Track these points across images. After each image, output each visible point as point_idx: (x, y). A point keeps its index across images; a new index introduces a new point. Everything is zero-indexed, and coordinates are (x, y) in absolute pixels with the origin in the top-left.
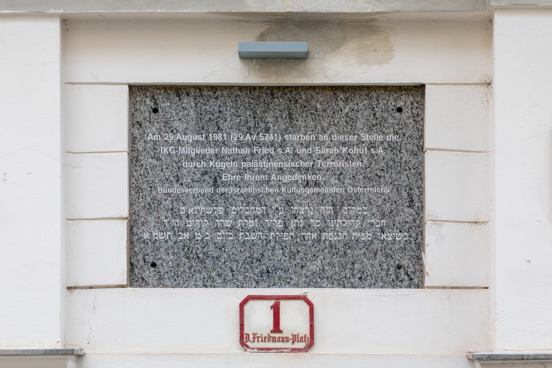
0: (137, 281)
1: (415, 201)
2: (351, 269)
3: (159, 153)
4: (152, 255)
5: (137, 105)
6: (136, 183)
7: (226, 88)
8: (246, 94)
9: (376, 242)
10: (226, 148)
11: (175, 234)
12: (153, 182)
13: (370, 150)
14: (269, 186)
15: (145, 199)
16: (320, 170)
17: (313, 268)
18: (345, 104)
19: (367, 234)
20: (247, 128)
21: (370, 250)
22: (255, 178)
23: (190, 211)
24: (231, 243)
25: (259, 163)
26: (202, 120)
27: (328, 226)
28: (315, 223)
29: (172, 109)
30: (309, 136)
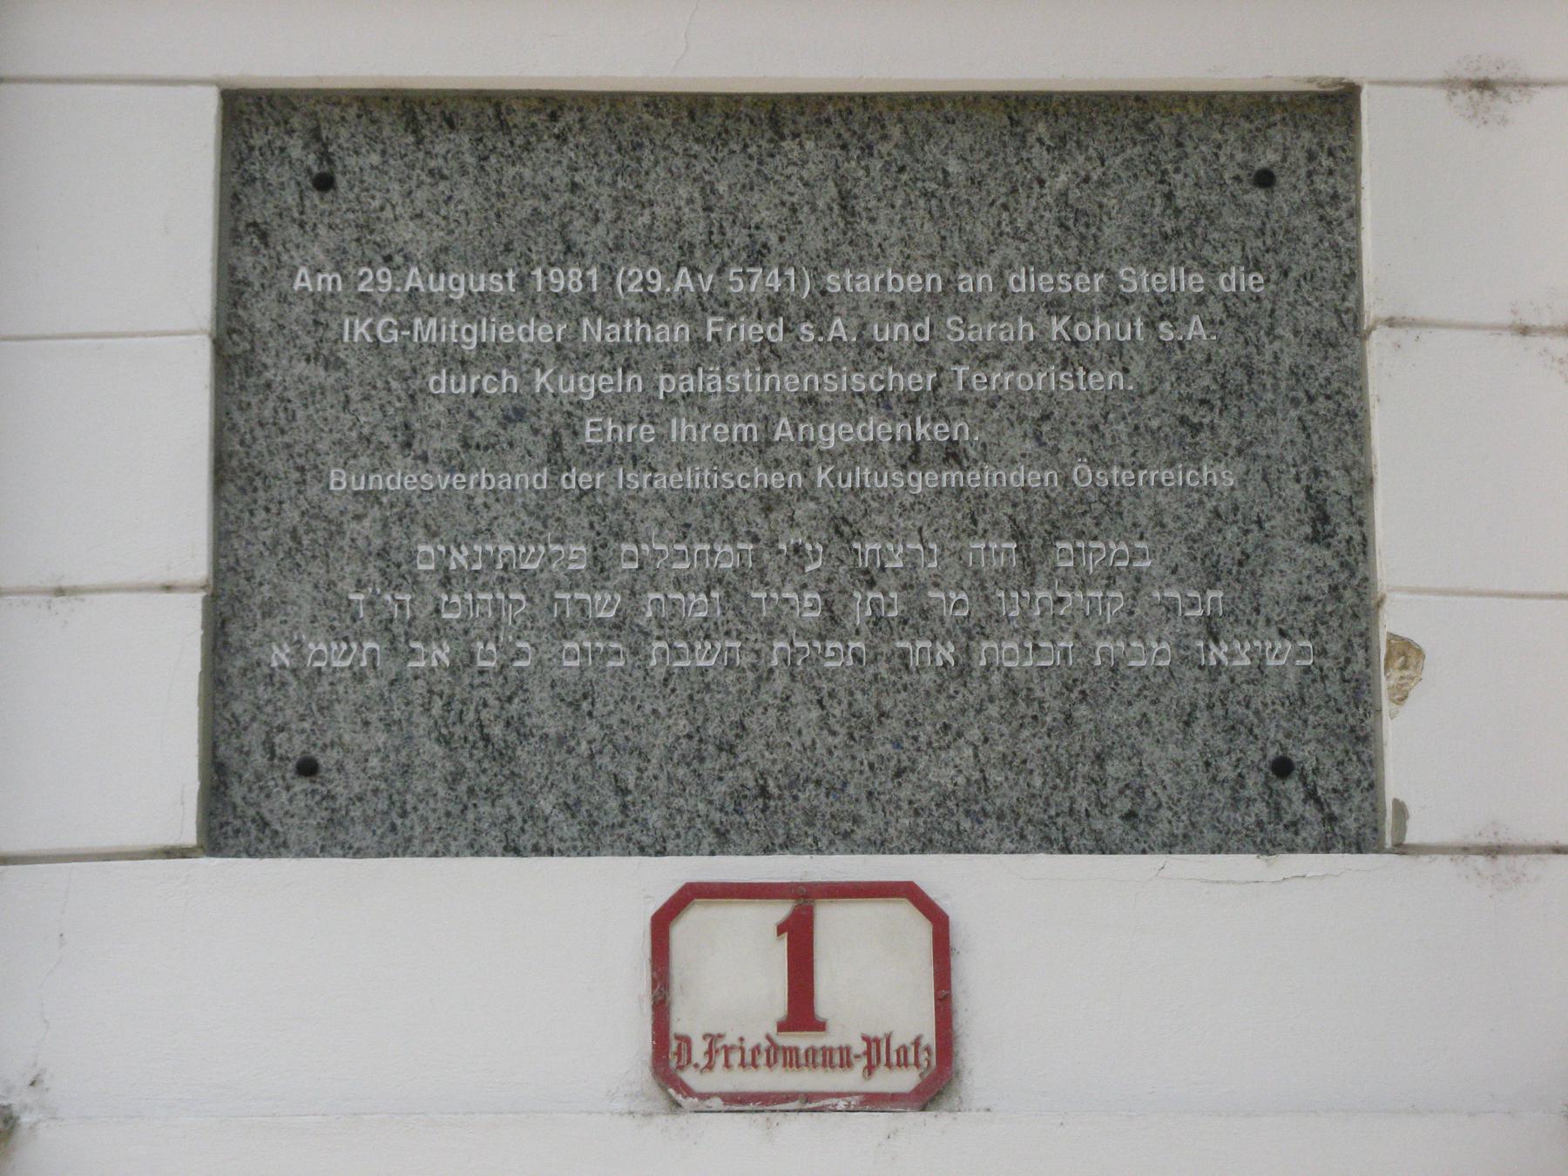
1: (1334, 520)
2: (1093, 780)
3: (336, 342)
4: (303, 731)
5: (253, 164)
6: (243, 455)
8: (676, 122)
9: (1190, 674)
10: (600, 320)
11: (395, 649)
12: (311, 448)
13: (1156, 329)
15: (279, 514)
16: (963, 402)
17: (943, 776)
18: (1054, 158)
19: (1154, 645)
20: (680, 248)
22: (709, 433)
23: (455, 559)
24: (615, 682)
25: (728, 378)
26: (504, 216)
27: (998, 613)
28: (949, 601)
29: (386, 178)
30: (918, 277)
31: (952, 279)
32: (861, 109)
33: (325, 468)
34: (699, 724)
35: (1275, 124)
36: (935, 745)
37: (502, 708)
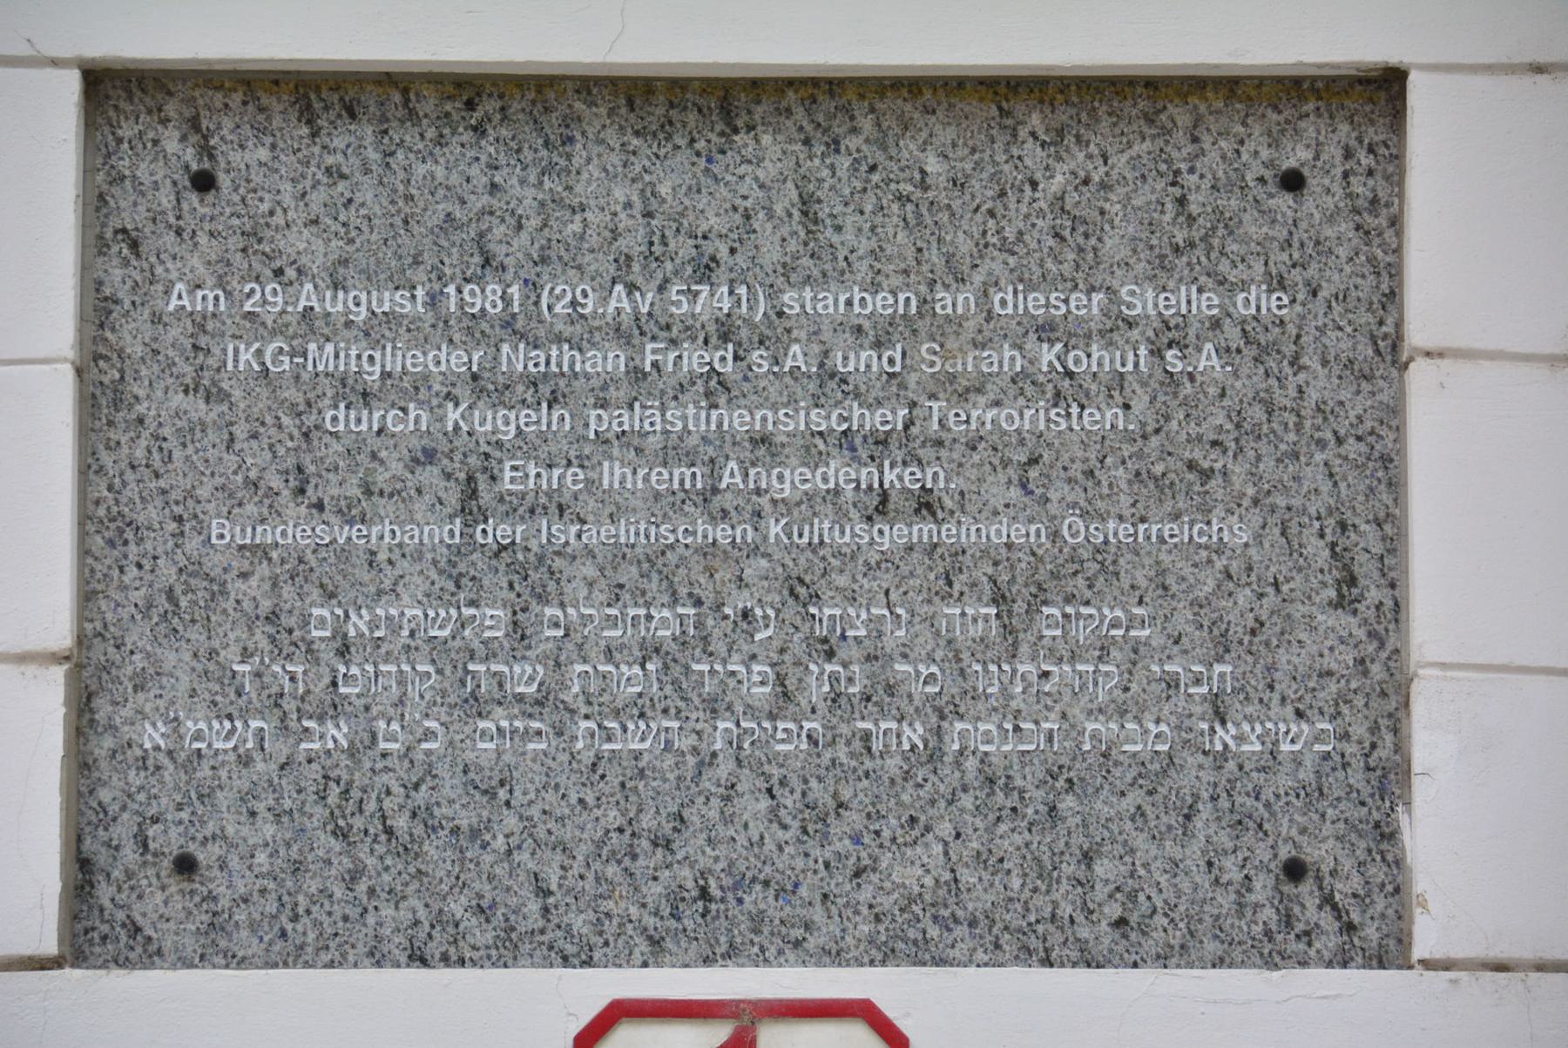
0: (104, 938)
1: (1362, 582)
3: (218, 370)
4: (180, 822)
5: (121, 159)
7: (520, 86)
8: (612, 112)
9: (1192, 760)
10: (522, 346)
11: (286, 728)
12: (190, 494)
13: (1162, 358)
14: (710, 514)
15: (152, 571)
16: (939, 443)
17: (908, 876)
18: (1049, 156)
19: (1151, 726)
20: (616, 260)
21: (1165, 797)
22: (646, 479)
23: (355, 625)
24: (537, 767)
25: (668, 414)
26: (412, 222)
27: (975, 689)
30: (889, 296)
31: (929, 298)
32: (827, 97)
33: (207, 518)
34: (632, 815)
35: (1307, 115)
36: (900, 840)
37: (408, 796)
